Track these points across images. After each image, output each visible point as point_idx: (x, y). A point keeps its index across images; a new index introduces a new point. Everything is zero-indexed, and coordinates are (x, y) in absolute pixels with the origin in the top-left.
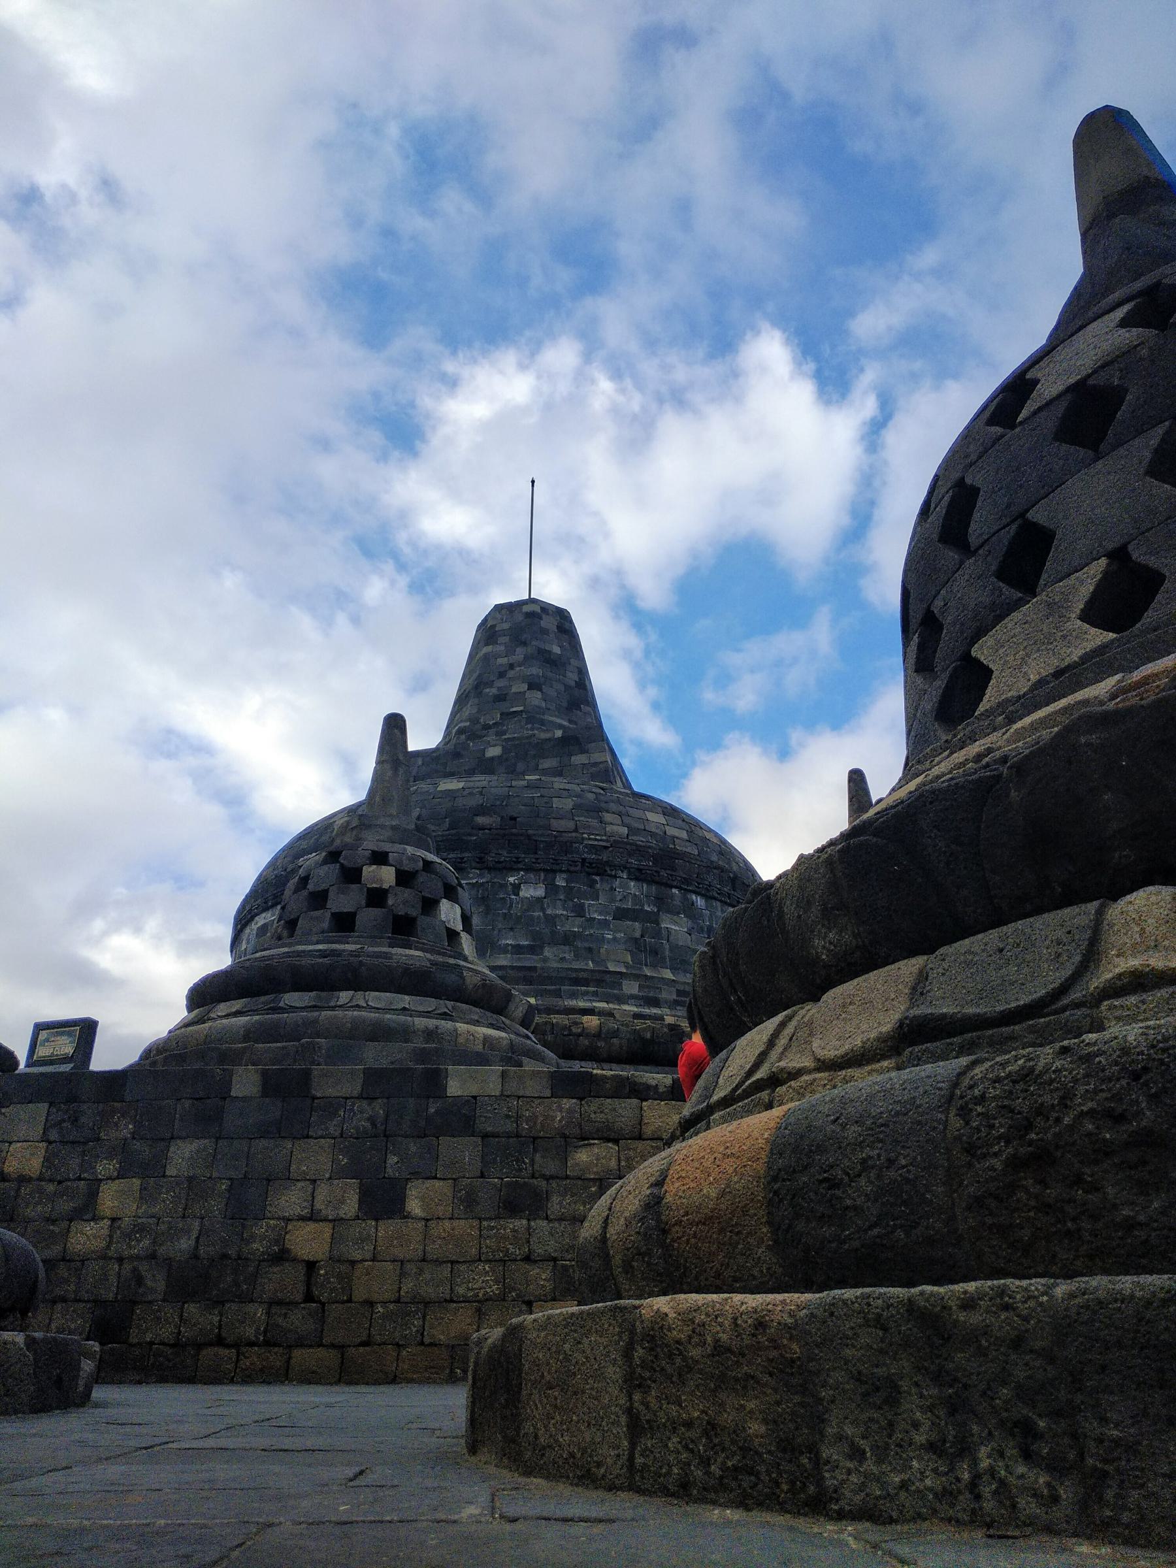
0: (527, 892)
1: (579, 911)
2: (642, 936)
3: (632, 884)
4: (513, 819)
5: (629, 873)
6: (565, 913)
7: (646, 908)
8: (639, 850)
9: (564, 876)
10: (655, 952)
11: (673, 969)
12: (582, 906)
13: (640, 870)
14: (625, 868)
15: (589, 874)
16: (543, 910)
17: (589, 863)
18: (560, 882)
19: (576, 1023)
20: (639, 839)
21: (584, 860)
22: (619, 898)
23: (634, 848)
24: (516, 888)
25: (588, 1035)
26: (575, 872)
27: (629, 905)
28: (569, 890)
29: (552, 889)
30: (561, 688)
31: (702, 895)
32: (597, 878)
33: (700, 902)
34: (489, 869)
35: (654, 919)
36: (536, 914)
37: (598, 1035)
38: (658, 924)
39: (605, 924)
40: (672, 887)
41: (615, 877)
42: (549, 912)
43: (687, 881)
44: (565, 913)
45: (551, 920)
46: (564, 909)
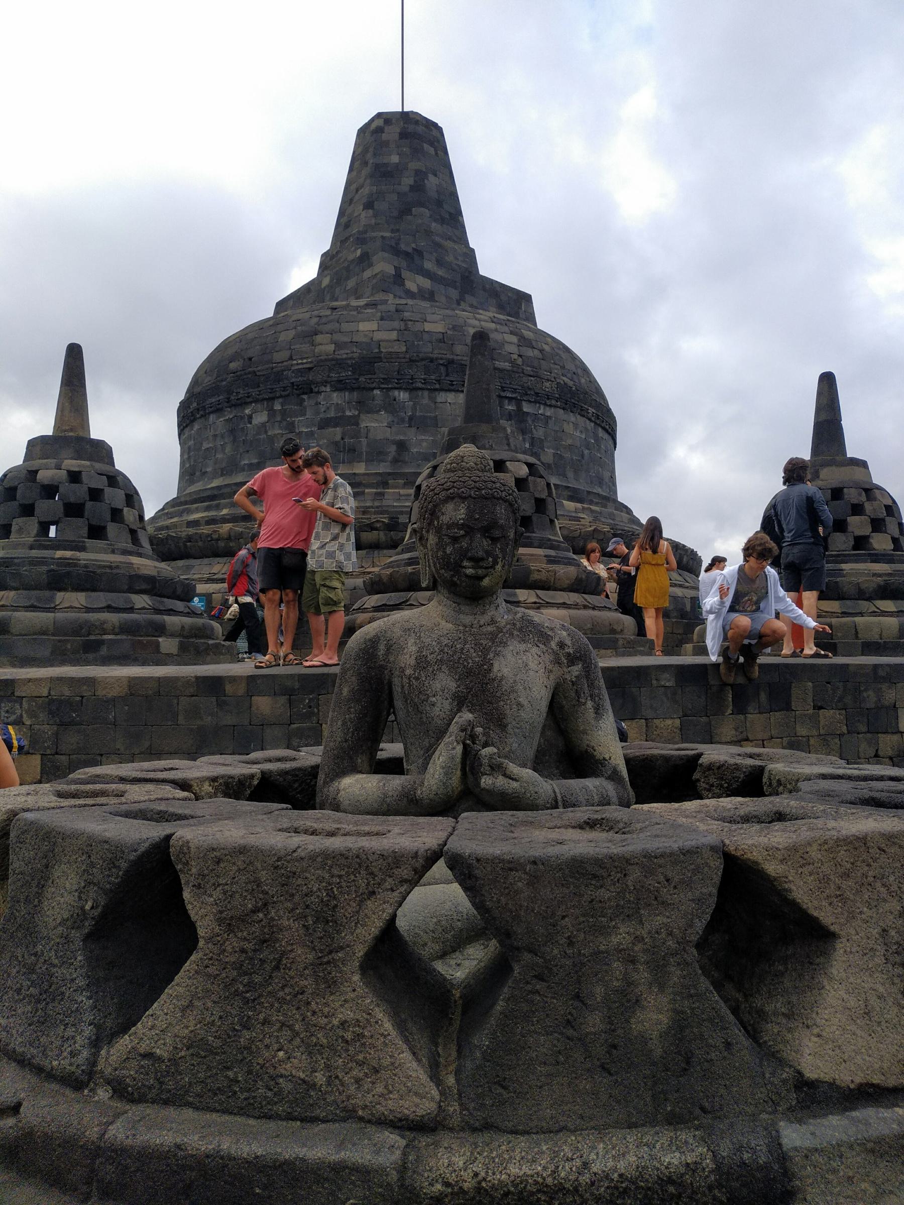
0: (260, 418)
1: (291, 427)
2: (342, 439)
3: (335, 395)
4: (250, 359)
5: (331, 386)
6: (280, 432)
7: (348, 413)
8: (339, 364)
9: (280, 400)
10: (352, 450)
11: (369, 461)
12: (293, 423)
13: (340, 381)
14: (326, 382)
15: (298, 395)
16: (266, 432)
17: (298, 386)
18: (277, 407)
19: (215, 531)
20: (343, 354)
21: (293, 383)
22: (323, 410)
23: (334, 362)
24: (250, 417)
25: (223, 539)
26: (288, 395)
27: (332, 414)
28: (284, 413)
29: (272, 412)
30: (395, 197)
31: (406, 389)
32: (305, 397)
33: (403, 396)
34: (235, 405)
35: (355, 421)
36: (262, 437)
37: (229, 538)
38: (357, 424)
39: (312, 434)
40: (373, 389)
41: (319, 393)
42: (269, 434)
43: (386, 380)
44: (280, 432)
45: (271, 439)
46: (280, 428)
